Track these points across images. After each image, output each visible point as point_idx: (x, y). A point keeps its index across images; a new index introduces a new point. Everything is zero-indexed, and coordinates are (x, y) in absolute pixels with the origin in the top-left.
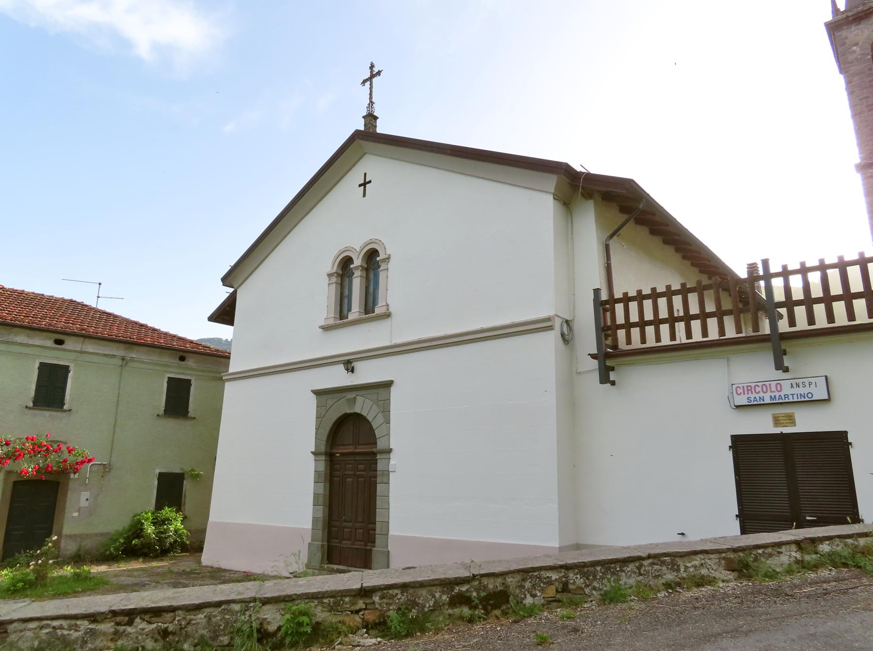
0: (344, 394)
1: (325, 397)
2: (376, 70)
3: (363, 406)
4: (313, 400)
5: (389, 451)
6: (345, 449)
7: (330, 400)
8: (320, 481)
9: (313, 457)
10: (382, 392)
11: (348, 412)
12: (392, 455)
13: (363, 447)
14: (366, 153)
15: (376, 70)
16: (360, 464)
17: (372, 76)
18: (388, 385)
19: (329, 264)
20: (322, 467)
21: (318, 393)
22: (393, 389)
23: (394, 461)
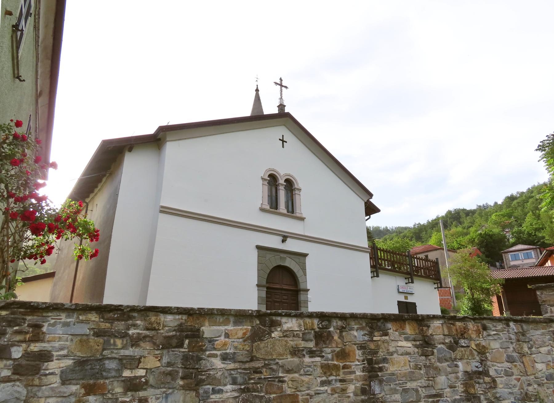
0: (278, 254)
1: (264, 252)
2: (279, 82)
3: (289, 263)
4: (255, 252)
5: (308, 290)
6: (274, 285)
7: (269, 255)
8: (263, 303)
9: (256, 288)
10: (301, 258)
11: (282, 264)
12: (309, 292)
13: (285, 286)
14: (284, 125)
15: (279, 82)
16: (284, 296)
17: (281, 85)
18: (305, 255)
19: (262, 172)
20: (264, 294)
21: (259, 248)
22: (307, 259)
23: (310, 295)
